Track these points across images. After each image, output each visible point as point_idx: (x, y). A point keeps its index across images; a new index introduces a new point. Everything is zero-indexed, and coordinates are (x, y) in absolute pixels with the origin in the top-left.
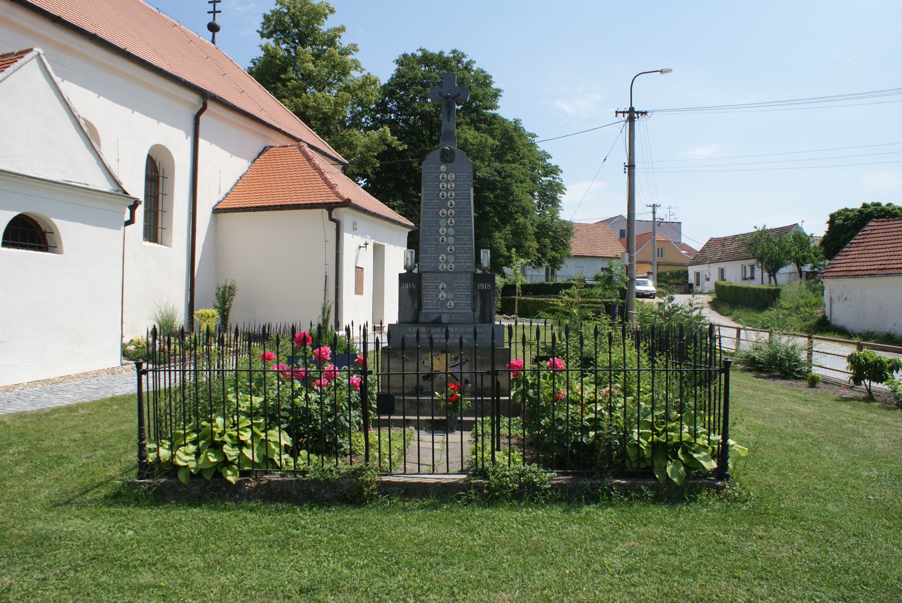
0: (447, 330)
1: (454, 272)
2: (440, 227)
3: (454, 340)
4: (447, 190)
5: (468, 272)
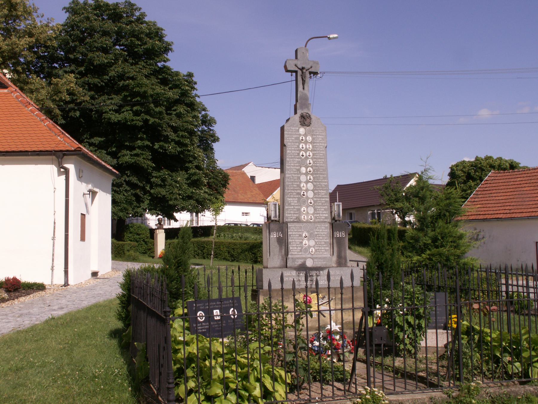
0: (329, 273)
1: (315, 222)
2: (300, 182)
3: (335, 283)
4: (306, 150)
5: (325, 222)
